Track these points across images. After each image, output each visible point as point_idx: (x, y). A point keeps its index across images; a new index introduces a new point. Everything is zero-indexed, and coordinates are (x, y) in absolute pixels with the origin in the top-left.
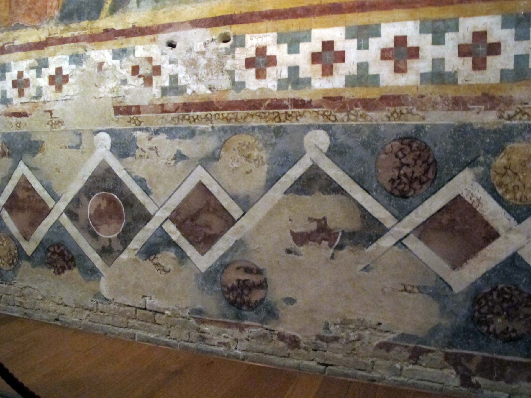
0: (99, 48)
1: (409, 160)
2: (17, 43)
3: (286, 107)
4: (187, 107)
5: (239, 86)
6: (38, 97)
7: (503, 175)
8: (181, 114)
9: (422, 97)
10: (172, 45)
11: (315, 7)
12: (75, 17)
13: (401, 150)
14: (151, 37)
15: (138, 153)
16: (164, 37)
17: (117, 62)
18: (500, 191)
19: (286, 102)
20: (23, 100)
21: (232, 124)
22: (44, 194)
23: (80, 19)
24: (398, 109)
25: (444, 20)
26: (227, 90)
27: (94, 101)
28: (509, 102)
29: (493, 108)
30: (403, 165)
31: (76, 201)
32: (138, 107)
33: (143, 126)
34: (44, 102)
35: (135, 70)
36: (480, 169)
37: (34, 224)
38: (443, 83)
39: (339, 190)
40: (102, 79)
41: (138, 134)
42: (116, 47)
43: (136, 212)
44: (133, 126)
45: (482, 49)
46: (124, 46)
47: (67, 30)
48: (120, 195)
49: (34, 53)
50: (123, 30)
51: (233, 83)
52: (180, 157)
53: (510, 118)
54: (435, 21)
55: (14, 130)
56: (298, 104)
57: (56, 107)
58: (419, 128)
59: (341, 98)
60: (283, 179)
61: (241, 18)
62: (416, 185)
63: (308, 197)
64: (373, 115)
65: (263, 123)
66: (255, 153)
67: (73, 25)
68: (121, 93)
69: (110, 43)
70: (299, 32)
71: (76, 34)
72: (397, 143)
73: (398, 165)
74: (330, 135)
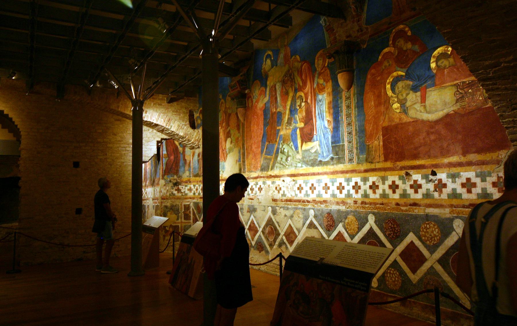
0: (269, 181)
1: (329, 220)
2: (251, 176)
3: (305, 202)
4: (287, 201)
5: (296, 195)
6: (256, 194)
7: (348, 225)
8: (286, 202)
9: (331, 201)
10: (284, 181)
11: (310, 173)
12: (264, 170)
13: (328, 216)
14: (279, 178)
15: (277, 214)
16: (282, 179)
17: (272, 185)
18: (348, 230)
19: (305, 201)
20: (253, 194)
21: (295, 207)
22: (257, 225)
23: (265, 171)
24: (327, 204)
25: (334, 179)
26: (294, 196)
27: (268, 196)
28: (347, 203)
29: (344, 205)
30: (328, 221)
31: (264, 228)
32: (277, 199)
33: (278, 205)
34: (257, 196)
35: (276, 188)
36: (343, 223)
37: (255, 235)
38: (334, 197)
39: (316, 228)
40: (269, 190)
41: (277, 208)
42: (272, 181)
43: (277, 233)
44: (276, 205)
45: (341, 188)
46: (274, 181)
47: (262, 174)
48: (274, 227)
49: (255, 180)
50: (273, 176)
51: (295, 194)
52: (285, 216)
53: (348, 208)
54: (332, 179)
55: (250, 204)
56: (308, 202)
57: (260, 197)
58: (331, 210)
59: (315, 200)
60: (306, 224)
61: (296, 175)
62: (331, 227)
63: (311, 230)
64: (322, 206)
65: (302, 207)
66: (300, 216)
67: (263, 173)
68: (273, 195)
69: (271, 179)
70: (307, 180)
71: (264, 175)
72: (327, 214)
73: (327, 221)
74: (314, 211)
